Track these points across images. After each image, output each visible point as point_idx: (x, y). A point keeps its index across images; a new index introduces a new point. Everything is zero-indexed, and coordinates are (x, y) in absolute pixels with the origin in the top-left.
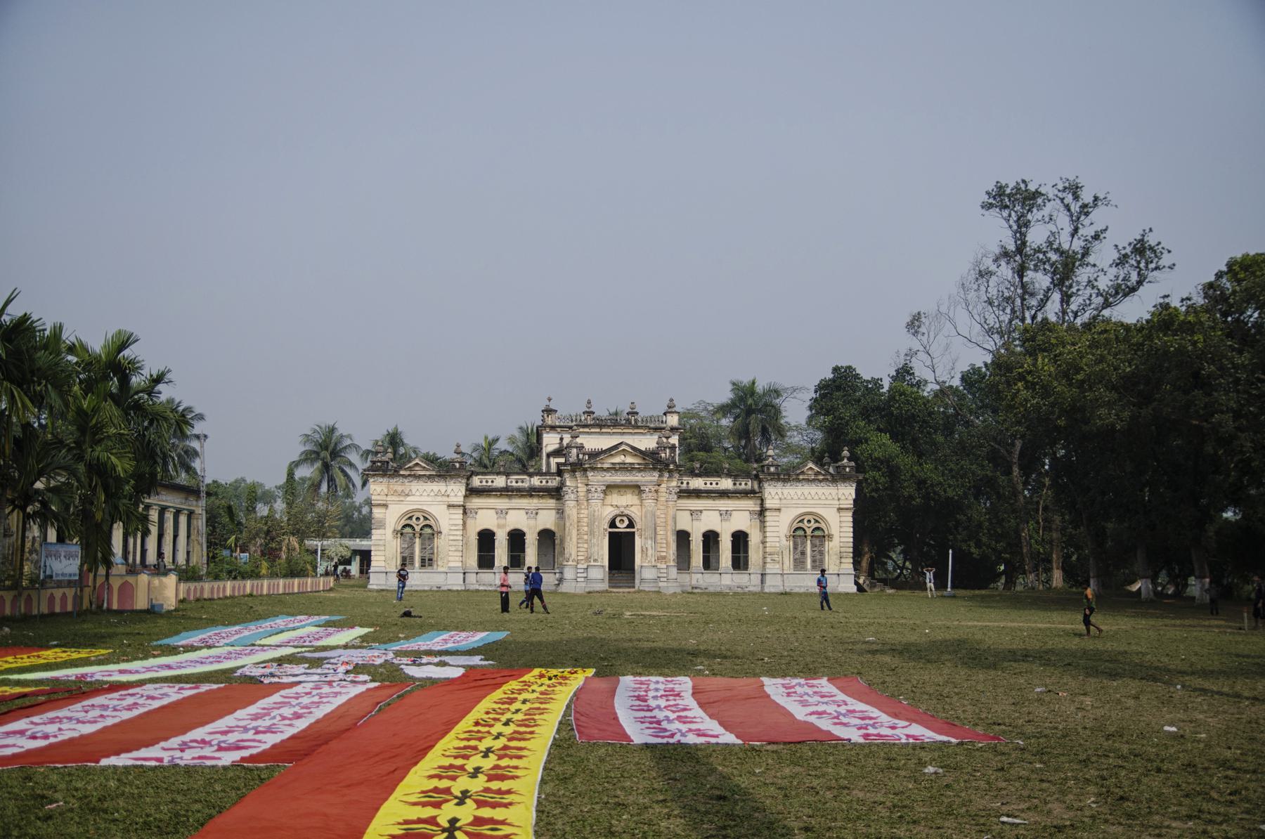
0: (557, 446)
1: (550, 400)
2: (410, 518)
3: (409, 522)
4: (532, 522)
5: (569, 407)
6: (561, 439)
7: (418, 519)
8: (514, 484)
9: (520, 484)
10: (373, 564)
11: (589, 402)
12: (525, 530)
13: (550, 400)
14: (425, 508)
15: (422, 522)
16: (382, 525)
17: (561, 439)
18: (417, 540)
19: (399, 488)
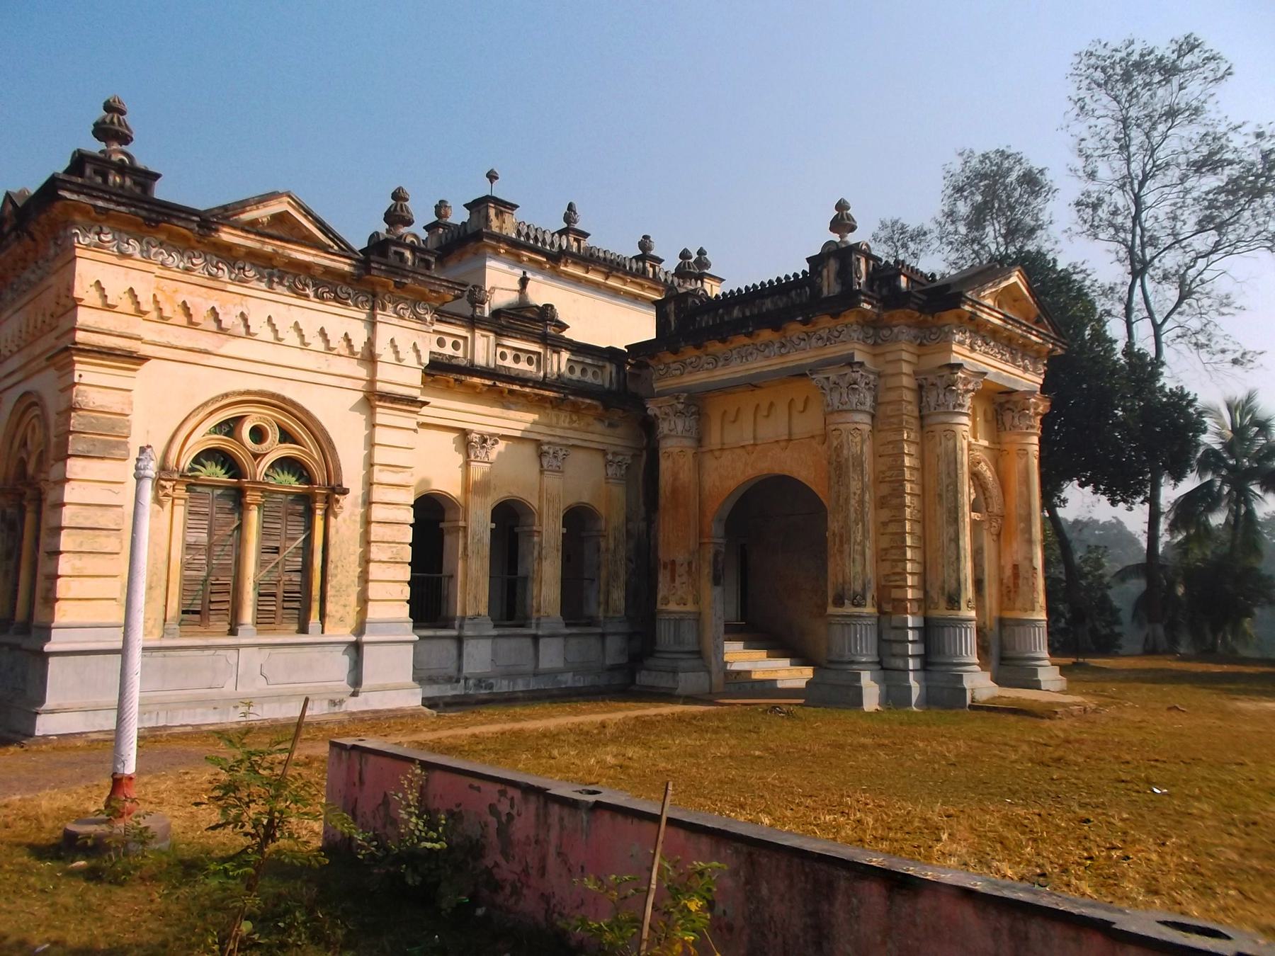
0: (513, 297)
1: (492, 176)
2: (230, 427)
3: (218, 441)
4: (553, 482)
5: (539, 214)
6: (524, 281)
7: (258, 434)
8: (509, 362)
9: (523, 366)
10: (64, 613)
11: (570, 207)
12: (534, 502)
13: (492, 176)
14: (289, 391)
15: (276, 450)
16: (110, 442)
17: (524, 281)
18: (254, 517)
19: (201, 302)
